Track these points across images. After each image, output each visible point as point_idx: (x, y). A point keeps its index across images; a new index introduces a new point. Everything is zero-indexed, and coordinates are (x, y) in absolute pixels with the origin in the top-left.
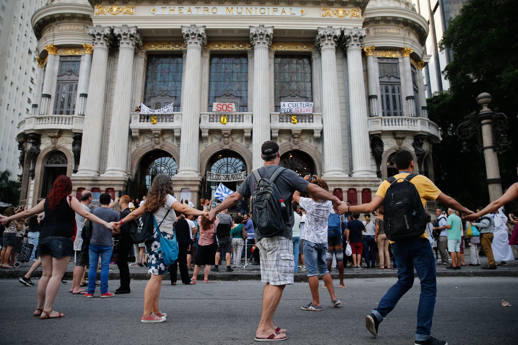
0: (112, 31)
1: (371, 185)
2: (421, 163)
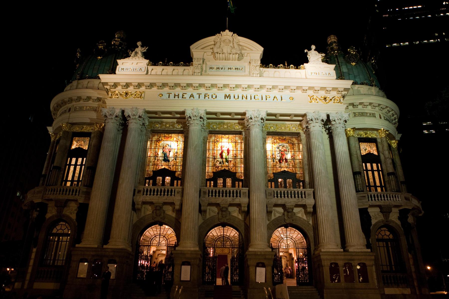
0: (123, 112)
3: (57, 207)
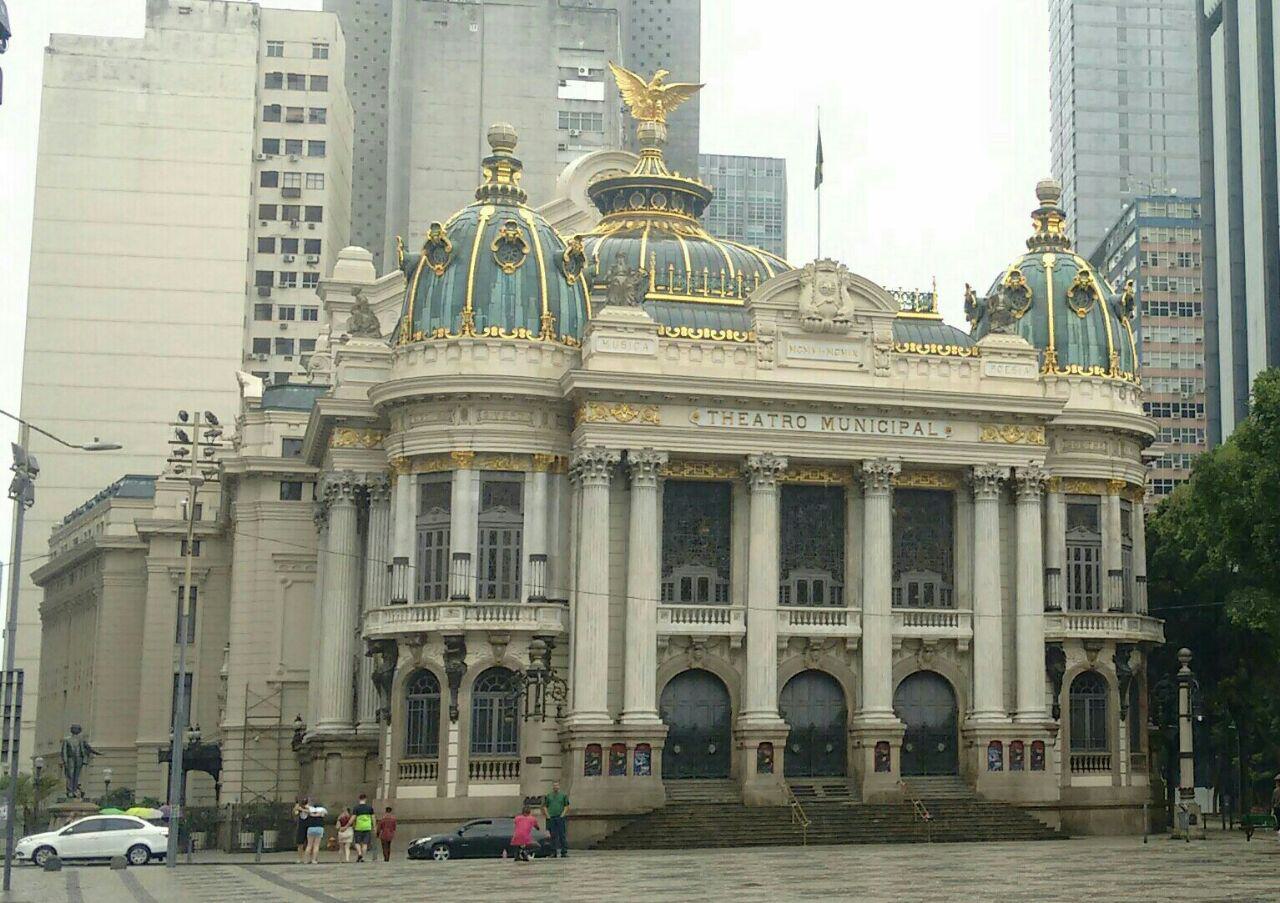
1: (1044, 736)
2: (1125, 693)
3: (493, 644)
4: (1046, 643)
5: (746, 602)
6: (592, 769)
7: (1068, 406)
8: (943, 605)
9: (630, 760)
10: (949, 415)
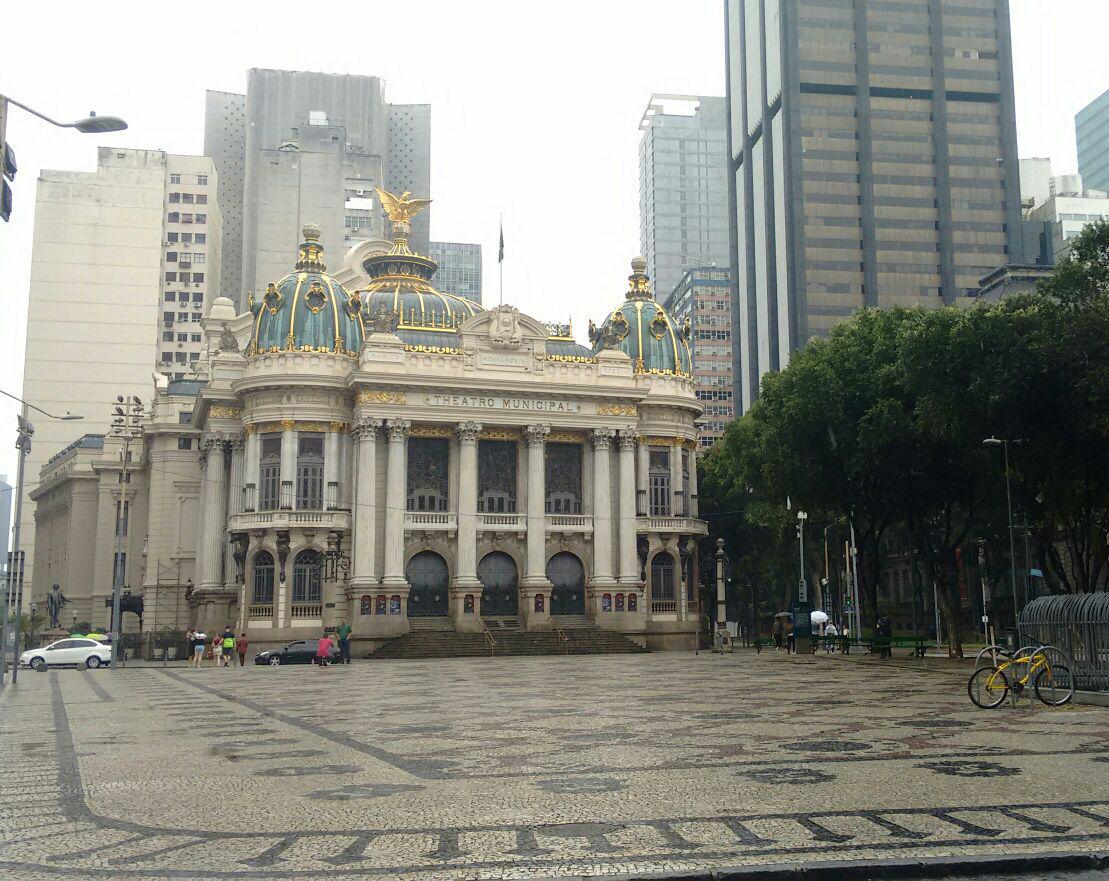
4: (638, 536)
5: (457, 511)
6: (365, 611)
7: (650, 393)
8: (575, 513)
9: (388, 605)
10: (579, 398)
